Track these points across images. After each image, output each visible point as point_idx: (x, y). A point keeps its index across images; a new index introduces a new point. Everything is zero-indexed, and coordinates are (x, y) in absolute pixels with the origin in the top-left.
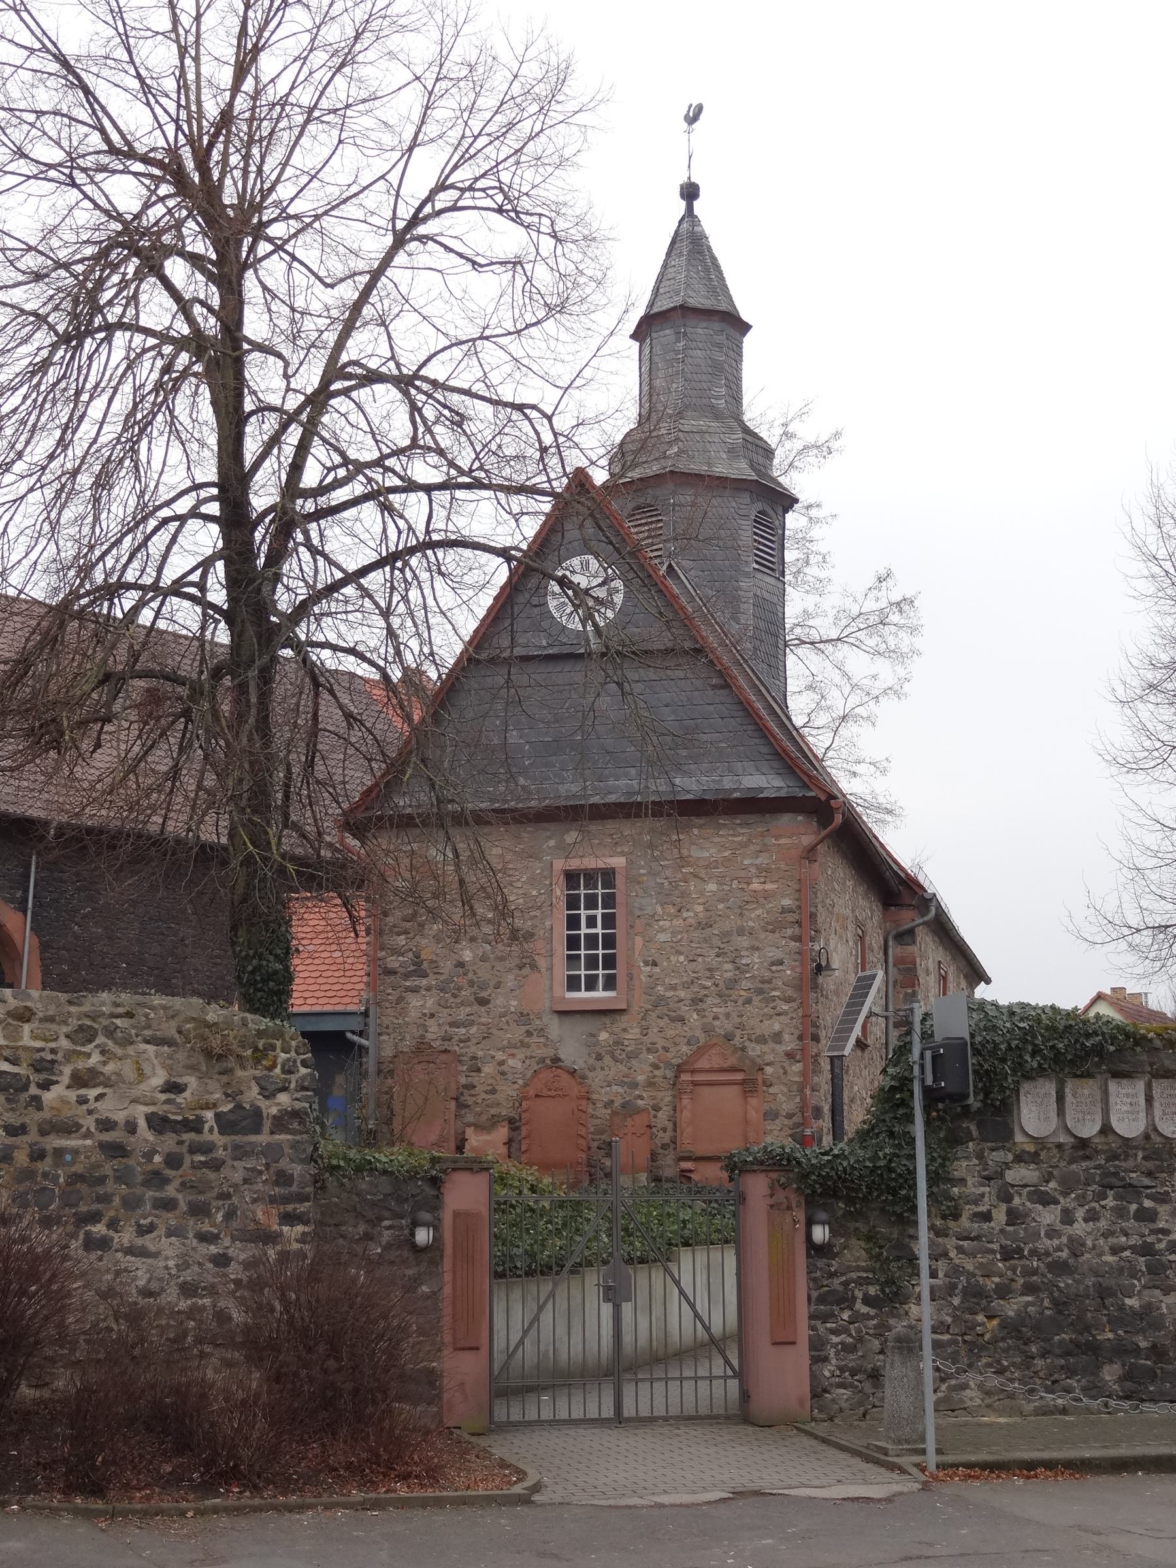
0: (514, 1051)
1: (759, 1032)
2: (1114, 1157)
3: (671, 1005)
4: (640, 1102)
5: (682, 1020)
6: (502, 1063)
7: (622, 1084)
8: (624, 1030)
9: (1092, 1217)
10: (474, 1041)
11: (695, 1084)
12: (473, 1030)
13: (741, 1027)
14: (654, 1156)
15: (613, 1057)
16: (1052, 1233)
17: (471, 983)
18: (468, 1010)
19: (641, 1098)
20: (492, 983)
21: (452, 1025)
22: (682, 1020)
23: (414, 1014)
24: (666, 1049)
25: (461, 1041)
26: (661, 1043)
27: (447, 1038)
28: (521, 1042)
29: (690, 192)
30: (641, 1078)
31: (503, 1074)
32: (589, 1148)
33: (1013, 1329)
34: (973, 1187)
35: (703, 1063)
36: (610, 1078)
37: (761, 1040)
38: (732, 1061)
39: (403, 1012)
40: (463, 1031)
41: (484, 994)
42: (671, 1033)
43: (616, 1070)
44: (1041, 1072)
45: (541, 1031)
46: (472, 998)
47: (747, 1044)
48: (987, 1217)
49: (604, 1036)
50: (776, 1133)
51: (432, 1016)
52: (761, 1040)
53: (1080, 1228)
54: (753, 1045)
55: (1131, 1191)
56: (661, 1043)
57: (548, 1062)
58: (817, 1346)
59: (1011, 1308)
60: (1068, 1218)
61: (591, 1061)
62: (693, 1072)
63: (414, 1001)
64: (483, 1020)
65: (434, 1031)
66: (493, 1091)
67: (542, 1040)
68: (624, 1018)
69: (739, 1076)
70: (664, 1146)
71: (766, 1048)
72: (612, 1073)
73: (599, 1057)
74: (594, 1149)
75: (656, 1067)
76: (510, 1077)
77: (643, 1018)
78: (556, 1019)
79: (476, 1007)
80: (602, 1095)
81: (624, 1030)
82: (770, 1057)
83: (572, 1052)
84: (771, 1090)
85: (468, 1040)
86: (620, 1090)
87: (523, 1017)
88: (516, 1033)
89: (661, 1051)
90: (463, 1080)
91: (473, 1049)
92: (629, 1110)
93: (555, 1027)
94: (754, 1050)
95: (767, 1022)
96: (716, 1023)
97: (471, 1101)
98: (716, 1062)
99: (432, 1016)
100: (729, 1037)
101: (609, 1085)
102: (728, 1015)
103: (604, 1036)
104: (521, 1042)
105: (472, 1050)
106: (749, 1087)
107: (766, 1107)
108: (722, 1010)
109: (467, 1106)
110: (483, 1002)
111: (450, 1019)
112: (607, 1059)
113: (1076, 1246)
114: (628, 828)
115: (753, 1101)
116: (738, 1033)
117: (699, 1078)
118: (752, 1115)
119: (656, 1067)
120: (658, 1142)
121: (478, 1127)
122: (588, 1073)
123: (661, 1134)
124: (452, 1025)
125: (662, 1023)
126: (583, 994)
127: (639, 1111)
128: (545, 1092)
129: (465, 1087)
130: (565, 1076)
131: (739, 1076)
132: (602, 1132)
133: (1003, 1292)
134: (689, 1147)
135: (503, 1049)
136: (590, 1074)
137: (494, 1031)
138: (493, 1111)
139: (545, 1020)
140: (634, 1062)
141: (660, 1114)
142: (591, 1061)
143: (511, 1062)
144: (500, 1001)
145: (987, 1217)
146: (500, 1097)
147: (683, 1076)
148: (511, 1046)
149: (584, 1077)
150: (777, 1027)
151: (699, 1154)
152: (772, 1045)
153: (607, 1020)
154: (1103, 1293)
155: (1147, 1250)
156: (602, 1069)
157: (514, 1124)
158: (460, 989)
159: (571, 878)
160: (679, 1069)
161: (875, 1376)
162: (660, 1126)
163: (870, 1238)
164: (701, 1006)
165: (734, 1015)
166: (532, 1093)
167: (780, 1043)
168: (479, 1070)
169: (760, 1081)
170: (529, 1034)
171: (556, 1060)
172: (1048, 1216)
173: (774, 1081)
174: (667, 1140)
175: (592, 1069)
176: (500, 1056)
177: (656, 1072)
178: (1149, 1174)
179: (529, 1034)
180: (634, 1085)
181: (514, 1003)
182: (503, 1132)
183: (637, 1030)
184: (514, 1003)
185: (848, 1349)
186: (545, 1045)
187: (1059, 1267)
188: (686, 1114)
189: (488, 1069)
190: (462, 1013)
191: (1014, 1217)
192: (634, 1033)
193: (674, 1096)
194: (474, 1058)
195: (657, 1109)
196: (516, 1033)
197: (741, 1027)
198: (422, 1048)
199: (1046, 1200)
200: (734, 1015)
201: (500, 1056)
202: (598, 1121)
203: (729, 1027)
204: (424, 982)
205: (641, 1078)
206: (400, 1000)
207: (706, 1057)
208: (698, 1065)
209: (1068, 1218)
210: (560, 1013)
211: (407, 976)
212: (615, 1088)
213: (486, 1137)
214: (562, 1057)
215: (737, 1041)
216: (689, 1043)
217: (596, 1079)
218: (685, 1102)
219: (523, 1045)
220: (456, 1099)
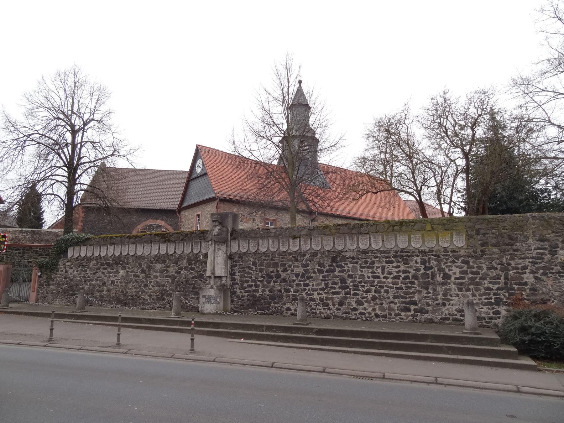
2: (82, 260)
9: (77, 271)
16: (71, 274)
29: (300, 82)
33: (64, 291)
34: (61, 266)
44: (71, 246)
48: (62, 271)
53: (75, 273)
55: (84, 266)
58: (38, 292)
59: (63, 287)
60: (74, 272)
113: (74, 276)
114: (201, 206)
133: (63, 284)
145: (62, 271)
154: (77, 285)
155: (84, 277)
159: (198, 215)
161: (45, 297)
163: (47, 274)
172: (71, 271)
178: (87, 263)
185: (42, 293)
187: (71, 280)
191: (66, 271)
199: (72, 268)
209: (74, 272)
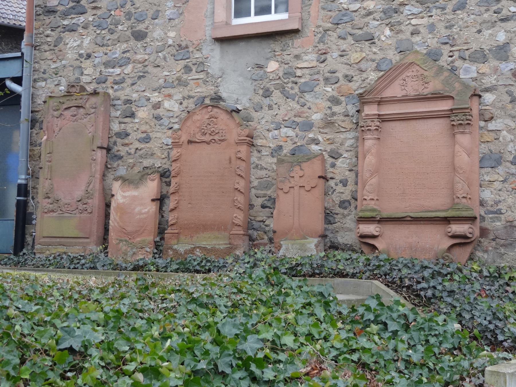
0: (172, 91)
1: (474, 46)
3: (358, 21)
4: (314, 148)
5: (371, 39)
6: (157, 106)
7: (293, 125)
8: (297, 57)
10: (129, 81)
11: (383, 119)
12: (128, 69)
13: (449, 41)
14: (329, 217)
15: (283, 91)
17: (129, 15)
18: (124, 46)
19: (316, 142)
20: (150, 13)
21: (107, 64)
22: (371, 39)
23: (71, 55)
24: (349, 79)
25: (116, 83)
26: (342, 70)
27: (101, 81)
28: (179, 79)
30: (316, 117)
31: (158, 118)
32: (251, 206)
35: (395, 90)
36: (279, 118)
37: (479, 57)
38: (435, 85)
39: (60, 56)
40: (118, 70)
41: (141, 27)
42: (355, 57)
43: (286, 108)
45: (201, 66)
46: (129, 33)
47: (458, 63)
49: (273, 66)
50: (497, 185)
51: (89, 56)
52: (479, 57)
54: (466, 65)
56: (342, 70)
57: (207, 101)
61: (258, 99)
62: (380, 103)
63: (72, 41)
64: (139, 57)
65: (89, 73)
66: (147, 140)
67: (202, 76)
68: (298, 42)
69: (444, 106)
70: (343, 204)
71: (485, 68)
72: (282, 112)
73: (267, 94)
74: (258, 208)
75: (335, 101)
76: (165, 121)
77: (321, 41)
78: (217, 48)
79: (133, 42)
80: (267, 140)
81: (297, 57)
82: (489, 81)
83: (236, 90)
84: (491, 126)
85: (123, 81)
86: (290, 132)
87: (182, 49)
88: (174, 69)
89: (342, 81)
90: (116, 127)
91: (128, 91)
92: (299, 156)
93: (216, 58)
94: (468, 72)
95: (487, 33)
96: (417, 39)
97: (123, 151)
98: (413, 88)
99: (89, 56)
100: (434, 56)
101: (278, 128)
102: (432, 28)
103: (273, 66)
104: (179, 79)
105: (126, 92)
106: (458, 119)
107: (484, 148)
108: (425, 21)
109: (121, 158)
110: (139, 36)
111: (105, 59)
112: (277, 96)
115: (464, 140)
116: (446, 49)
117: (388, 110)
118: (463, 159)
119: (335, 101)
120: (336, 198)
121: (125, 180)
122: (254, 115)
123: (340, 188)
124: (107, 64)
125: (344, 45)
126: (253, 19)
127: (310, 157)
128: (199, 137)
129: (118, 135)
130: (223, 116)
131: (444, 106)
132: (267, 187)
134: (372, 205)
135: (158, 89)
136: (255, 115)
137: (150, 69)
138: (147, 163)
139: (206, 51)
140: (307, 96)
141: (339, 163)
142: (258, 99)
143: (167, 104)
144: (157, 33)
146: (154, 146)
147: (371, 109)
148: (168, 84)
149: (248, 119)
150: (502, 37)
151: (385, 215)
152: (494, 63)
153: (276, 46)
156: (270, 107)
157: (164, 175)
158: (116, 24)
160: (363, 99)
162: (338, 178)
164: (396, 18)
165: (441, 27)
166: (184, 138)
167: (506, 59)
168: (132, 115)
169: (475, 112)
170: (187, 69)
171: (217, 99)
173: (496, 112)
174: (347, 196)
175: (258, 108)
176: (155, 97)
177: (336, 109)
179: (187, 69)
180: (308, 126)
181: (172, 34)
182: (151, 187)
183: (313, 57)
184: (172, 34)
186: (205, 82)
188: (370, 160)
189: (142, 114)
190: (117, 52)
192: (310, 59)
193: (357, 139)
194: (128, 102)
195: (335, 155)
196: (174, 69)
197: (449, 41)
198: (75, 89)
200: (441, 27)
201: (155, 97)
202: (263, 173)
203: (433, 42)
204: (82, 18)
205: (316, 117)
206: (59, 40)
207: (399, 81)
208: (388, 93)
210: (222, 41)
211: (65, 15)
212: (284, 130)
213: (132, 193)
214: (224, 95)
215: (444, 61)
216: (378, 69)
217: (262, 120)
218: (369, 143)
219: (181, 83)
220: (108, 150)
